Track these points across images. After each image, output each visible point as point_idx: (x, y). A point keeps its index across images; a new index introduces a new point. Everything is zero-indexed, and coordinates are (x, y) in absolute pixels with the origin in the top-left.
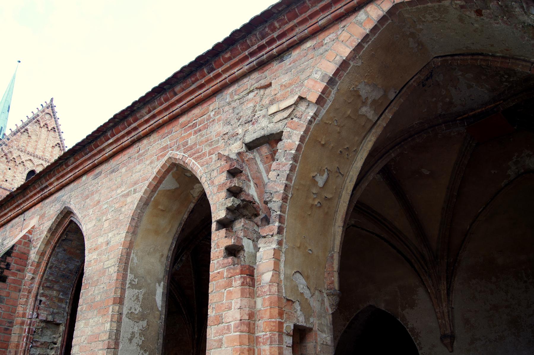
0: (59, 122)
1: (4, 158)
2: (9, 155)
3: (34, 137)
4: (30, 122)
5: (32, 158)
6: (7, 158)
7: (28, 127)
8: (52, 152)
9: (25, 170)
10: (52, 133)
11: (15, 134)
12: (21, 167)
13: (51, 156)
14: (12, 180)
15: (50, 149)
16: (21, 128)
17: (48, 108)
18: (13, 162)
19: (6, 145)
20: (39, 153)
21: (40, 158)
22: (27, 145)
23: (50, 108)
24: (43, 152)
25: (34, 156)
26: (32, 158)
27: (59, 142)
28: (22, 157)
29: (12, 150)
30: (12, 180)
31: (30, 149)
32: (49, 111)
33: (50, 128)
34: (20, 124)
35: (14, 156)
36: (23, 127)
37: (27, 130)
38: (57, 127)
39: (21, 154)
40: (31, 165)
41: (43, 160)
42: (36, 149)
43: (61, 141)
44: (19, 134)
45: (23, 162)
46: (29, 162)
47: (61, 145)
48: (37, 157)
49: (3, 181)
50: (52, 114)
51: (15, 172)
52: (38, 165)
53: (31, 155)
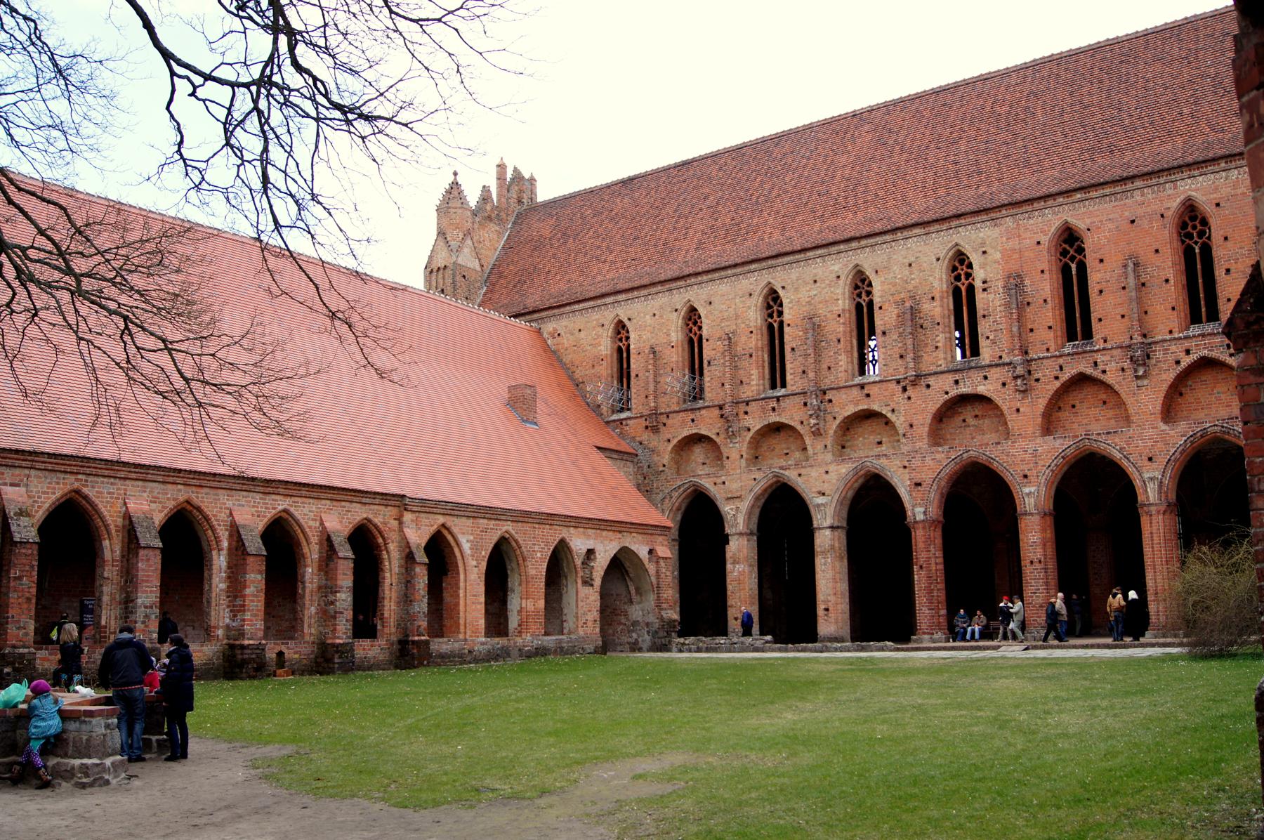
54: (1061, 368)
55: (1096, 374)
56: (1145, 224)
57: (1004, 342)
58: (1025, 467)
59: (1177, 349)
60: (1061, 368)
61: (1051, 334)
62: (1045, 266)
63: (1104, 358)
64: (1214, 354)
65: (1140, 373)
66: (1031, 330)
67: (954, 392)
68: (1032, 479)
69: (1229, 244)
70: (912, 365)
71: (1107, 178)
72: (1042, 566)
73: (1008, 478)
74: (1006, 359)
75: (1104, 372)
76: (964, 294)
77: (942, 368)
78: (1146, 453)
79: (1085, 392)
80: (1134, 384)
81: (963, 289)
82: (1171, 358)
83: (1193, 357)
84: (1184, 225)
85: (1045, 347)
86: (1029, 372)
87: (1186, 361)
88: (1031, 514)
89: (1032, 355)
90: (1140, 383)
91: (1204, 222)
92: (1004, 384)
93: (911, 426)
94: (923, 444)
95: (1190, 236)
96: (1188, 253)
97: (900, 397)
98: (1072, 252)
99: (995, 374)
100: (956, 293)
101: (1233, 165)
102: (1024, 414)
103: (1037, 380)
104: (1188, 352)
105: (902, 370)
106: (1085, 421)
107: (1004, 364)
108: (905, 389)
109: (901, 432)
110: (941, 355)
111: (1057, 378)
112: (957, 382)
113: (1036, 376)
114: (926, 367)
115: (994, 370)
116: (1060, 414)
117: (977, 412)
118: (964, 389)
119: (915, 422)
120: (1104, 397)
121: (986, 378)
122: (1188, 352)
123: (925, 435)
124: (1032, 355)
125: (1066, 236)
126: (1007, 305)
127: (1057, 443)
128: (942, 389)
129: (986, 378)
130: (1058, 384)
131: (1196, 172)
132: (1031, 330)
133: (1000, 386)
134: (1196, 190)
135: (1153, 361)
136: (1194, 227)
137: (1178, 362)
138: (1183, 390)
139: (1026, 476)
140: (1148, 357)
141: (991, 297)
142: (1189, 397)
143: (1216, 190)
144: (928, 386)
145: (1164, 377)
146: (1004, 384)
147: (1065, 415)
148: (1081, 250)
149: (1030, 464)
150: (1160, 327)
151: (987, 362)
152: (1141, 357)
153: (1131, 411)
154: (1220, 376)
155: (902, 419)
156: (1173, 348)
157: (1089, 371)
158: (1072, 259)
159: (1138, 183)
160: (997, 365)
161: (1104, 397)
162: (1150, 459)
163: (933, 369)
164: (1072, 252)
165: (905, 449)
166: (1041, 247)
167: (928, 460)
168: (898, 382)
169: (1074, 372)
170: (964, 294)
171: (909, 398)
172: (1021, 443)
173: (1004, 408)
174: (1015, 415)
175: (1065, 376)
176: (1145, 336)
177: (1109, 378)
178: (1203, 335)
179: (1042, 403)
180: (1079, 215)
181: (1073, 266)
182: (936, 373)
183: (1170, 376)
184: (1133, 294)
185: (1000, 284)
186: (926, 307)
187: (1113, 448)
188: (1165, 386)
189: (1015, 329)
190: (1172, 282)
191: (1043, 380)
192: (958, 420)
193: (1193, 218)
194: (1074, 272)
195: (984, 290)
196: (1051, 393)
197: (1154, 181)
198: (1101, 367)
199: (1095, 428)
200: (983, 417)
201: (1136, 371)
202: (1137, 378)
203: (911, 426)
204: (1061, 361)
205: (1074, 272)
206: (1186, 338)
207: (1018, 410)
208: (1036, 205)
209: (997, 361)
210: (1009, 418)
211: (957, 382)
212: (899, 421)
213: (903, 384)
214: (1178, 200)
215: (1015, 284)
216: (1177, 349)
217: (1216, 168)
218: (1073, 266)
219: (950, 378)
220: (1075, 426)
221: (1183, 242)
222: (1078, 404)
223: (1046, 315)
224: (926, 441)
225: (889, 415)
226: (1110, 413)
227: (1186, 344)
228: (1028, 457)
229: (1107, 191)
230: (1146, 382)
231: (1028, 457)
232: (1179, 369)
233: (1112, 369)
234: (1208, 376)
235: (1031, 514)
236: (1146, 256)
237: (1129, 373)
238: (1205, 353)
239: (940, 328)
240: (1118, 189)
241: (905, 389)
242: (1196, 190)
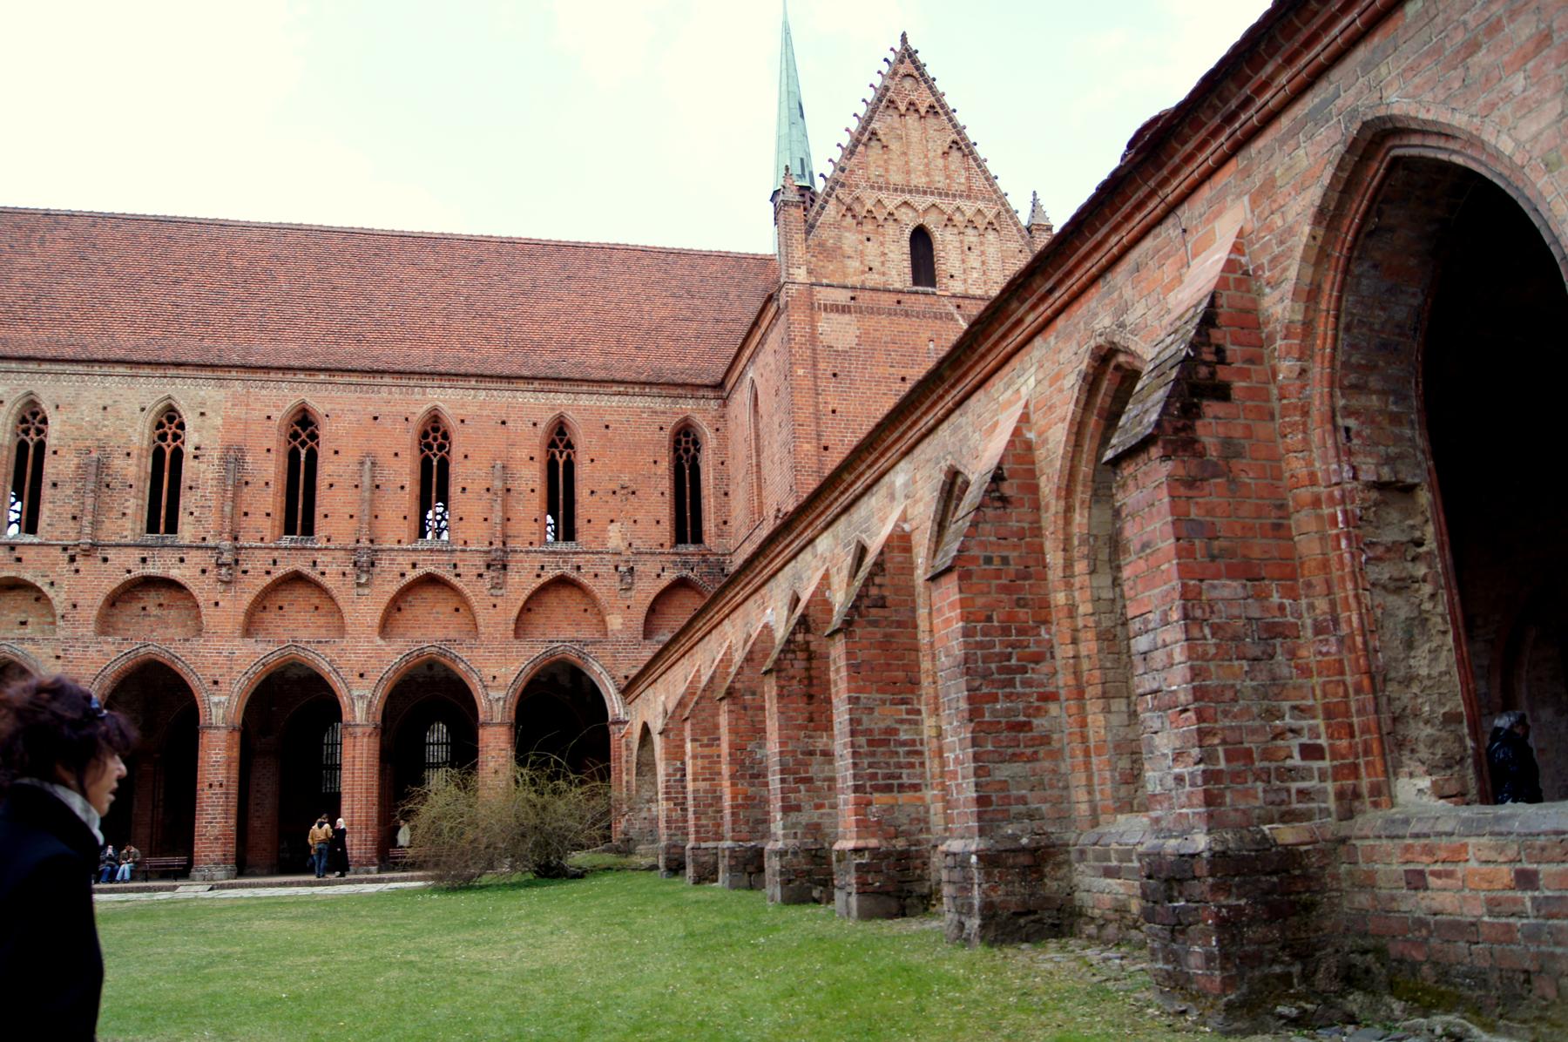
0: (940, 86)
1: (849, 219)
2: (857, 207)
3: (895, 146)
4: (874, 111)
5: (907, 197)
6: (854, 217)
7: (875, 125)
8: (946, 168)
9: (902, 232)
10: (931, 120)
11: (852, 153)
12: (891, 228)
13: (948, 177)
14: (883, 264)
15: (940, 162)
16: (861, 134)
17: (902, 62)
18: (870, 221)
19: (843, 185)
20: (919, 180)
21: (925, 193)
22: (887, 170)
23: (907, 60)
24: (928, 175)
25: (910, 192)
26: (907, 197)
27: (955, 137)
28: (886, 202)
29: (857, 192)
30: (883, 264)
31: (896, 178)
32: (907, 67)
33: (923, 111)
34: (854, 125)
35: (869, 206)
36: (864, 129)
37: (874, 133)
38: (938, 101)
39: (882, 195)
40: (911, 214)
41: (932, 194)
42: (908, 172)
43: (959, 133)
44: (861, 148)
45: (891, 214)
46: (903, 210)
47: (962, 144)
48: (918, 191)
49: (863, 272)
50: (916, 73)
51: (882, 244)
52: (926, 211)
53: (903, 191)
54: (275, 562)
55: (313, 574)
56: (387, 423)
57: (211, 521)
58: (217, 672)
59: (404, 561)
60: (275, 562)
61: (269, 522)
62: (273, 445)
63: (325, 559)
64: (440, 572)
65: (363, 581)
66: (246, 514)
67: (139, 571)
68: (223, 686)
69: (468, 463)
70: (88, 530)
71: (355, 365)
72: (223, 790)
73: (193, 682)
74: (211, 542)
76: (168, 457)
77: (128, 540)
78: (358, 669)
79: (296, 594)
80: (354, 592)
81: (168, 451)
82: (397, 570)
83: (419, 572)
84: (425, 435)
85: (259, 536)
86: (237, 561)
87: (412, 575)
88: (217, 728)
89: (243, 542)
90: (360, 591)
91: (445, 436)
92: (204, 571)
93: (75, 606)
94: (89, 631)
95: (430, 447)
96: (426, 464)
97: (64, 566)
98: (304, 436)
99: (194, 557)
100: (158, 454)
101: (483, 385)
102: (225, 608)
103: (245, 572)
104: (414, 566)
105: (73, 535)
106: (292, 627)
107: (207, 548)
108: (72, 559)
109: (59, 612)
110: (129, 525)
111: (268, 573)
112: (144, 560)
113: (245, 567)
114: (104, 538)
115: (193, 553)
116: (264, 615)
117: (162, 601)
118: (152, 570)
119: (81, 602)
120: (317, 601)
121: (182, 560)
122: (414, 566)
123: (92, 619)
124: (243, 542)
125: (299, 417)
126: (222, 481)
127: (259, 648)
128: (124, 565)
129: (182, 560)
130: (268, 580)
131: (447, 384)
132: (246, 514)
133: (198, 573)
134: (444, 402)
135: (377, 570)
136: (435, 439)
137: (403, 575)
138: (402, 606)
139: (216, 683)
140: (373, 564)
141: (203, 467)
142: (408, 613)
143: (463, 406)
144: (105, 560)
145: (387, 588)
146: (204, 571)
147: (270, 616)
148: (314, 437)
149: (222, 670)
150: (390, 535)
151: (187, 542)
152: (365, 564)
153: (347, 620)
154: (442, 596)
155: (63, 596)
156: (400, 559)
157: (306, 570)
158: (303, 444)
159: (387, 380)
160: (198, 548)
161: (317, 601)
162: (361, 675)
163: (116, 539)
164: (304, 436)
165: (61, 634)
166: (271, 423)
167: (92, 652)
168: (65, 549)
169: (290, 568)
170: (168, 457)
171: (77, 571)
172: (215, 643)
173: (201, 599)
174: (213, 608)
175: (279, 572)
176: (372, 541)
177: (327, 582)
178: (431, 551)
179: (247, 599)
180: (322, 398)
181: (303, 452)
182: (118, 545)
183: (394, 588)
184: (367, 494)
185: (216, 454)
186: (118, 462)
187: (323, 660)
188: (387, 598)
189: (227, 509)
190: (407, 489)
191: (251, 572)
192: (136, 607)
193: (436, 430)
194: (303, 458)
195: (196, 457)
196: (259, 589)
197: (404, 382)
198: (320, 568)
199: (303, 635)
200: (170, 607)
201: (358, 577)
202: (359, 585)
203: (75, 606)
204: (276, 554)
205: (303, 458)
206: (414, 550)
207: (217, 604)
208: (272, 375)
210: (204, 611)
211: (144, 560)
212: (59, 598)
213: (71, 552)
214: (425, 407)
215: (234, 458)
216: (404, 561)
217: (466, 384)
218: (303, 452)
219: (137, 554)
220: (280, 630)
221: (422, 451)
222: (286, 606)
223: (267, 500)
224: (92, 627)
225: (45, 589)
226: (322, 621)
227: (414, 557)
228: (221, 660)
229: (354, 379)
230: (366, 591)
231: (221, 660)
232: (404, 582)
233: (332, 571)
234: (429, 594)
235: (217, 728)
236: (385, 457)
237: (351, 579)
238: (431, 569)
239: (133, 491)
240: (366, 380)
241: (72, 559)
242: (444, 402)
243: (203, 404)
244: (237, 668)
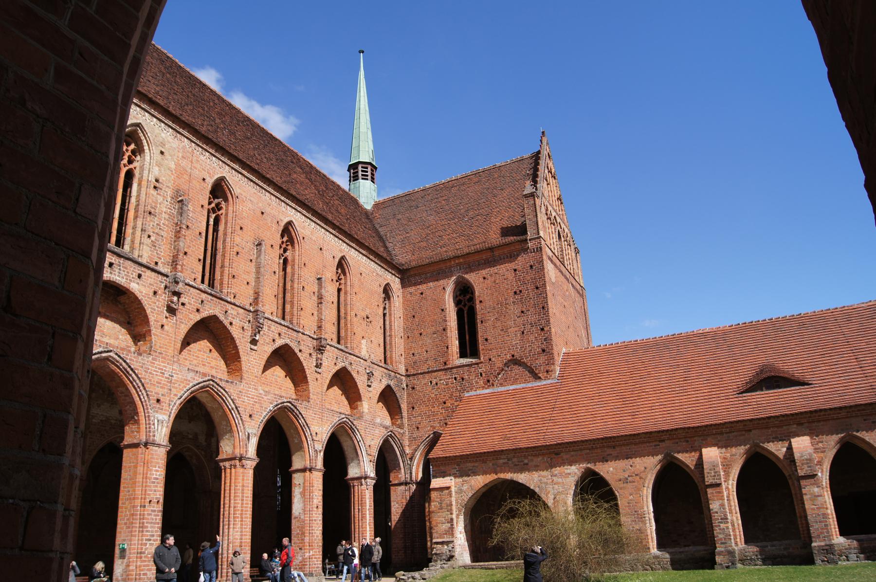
68: (165, 406)
75: (231, 324)
85: (193, 276)
88: (159, 445)
103: (183, 304)
106: (195, 362)
115: (149, 273)
133: (152, 294)
146: (155, 293)
174: (160, 330)
177: (235, 332)
179: (184, 329)
191: (187, 306)
196: (192, 323)
207: (162, 326)
209: (152, 266)
235: (159, 445)
243: (163, 144)
244: (174, 391)
